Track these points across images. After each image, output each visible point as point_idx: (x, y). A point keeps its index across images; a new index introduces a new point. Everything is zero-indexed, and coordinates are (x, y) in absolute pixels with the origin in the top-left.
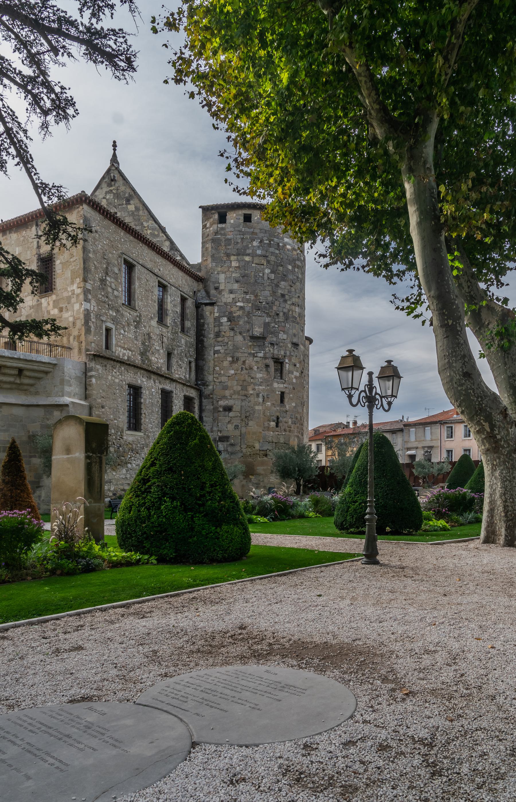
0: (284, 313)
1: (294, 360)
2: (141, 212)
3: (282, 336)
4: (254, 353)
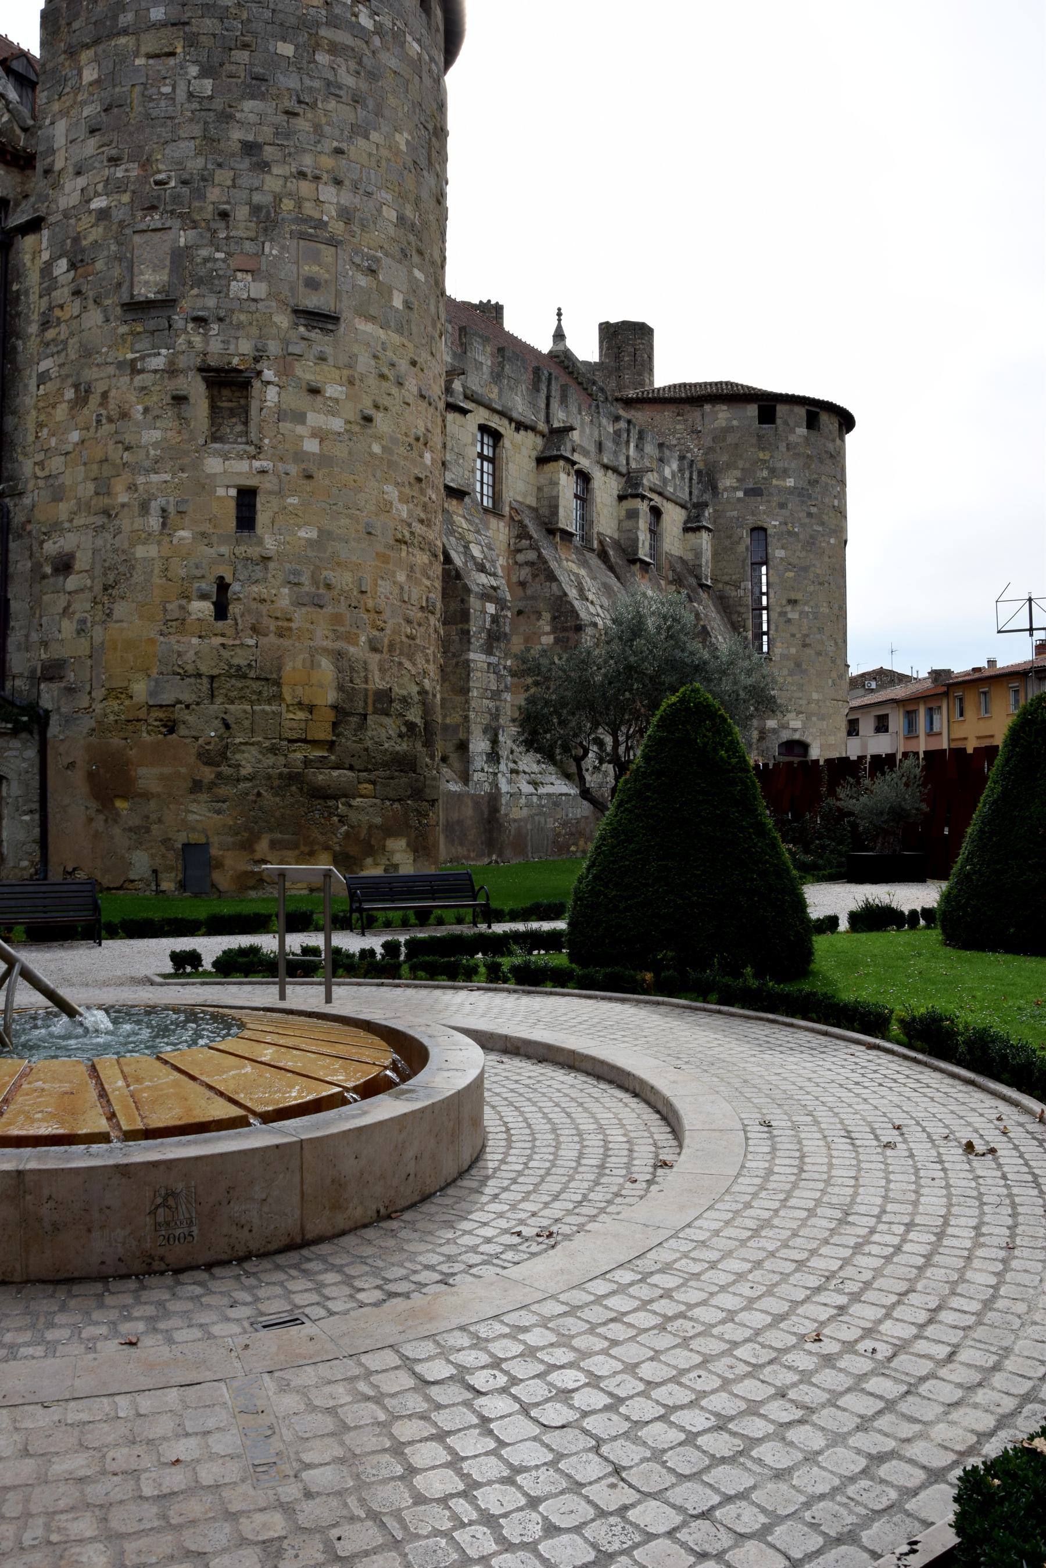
0: (256, 210)
1: (307, 372)
3: (242, 286)
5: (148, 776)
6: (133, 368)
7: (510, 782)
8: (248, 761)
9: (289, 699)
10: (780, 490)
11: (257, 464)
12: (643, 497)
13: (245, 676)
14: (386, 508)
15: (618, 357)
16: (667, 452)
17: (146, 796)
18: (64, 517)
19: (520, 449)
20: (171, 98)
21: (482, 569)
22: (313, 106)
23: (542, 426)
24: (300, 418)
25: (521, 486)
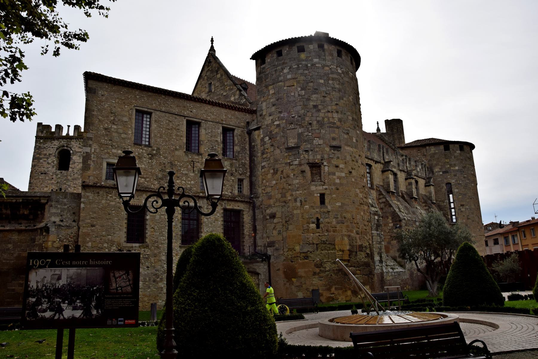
0: (318, 122)
1: (334, 162)
2: (224, 77)
4: (290, 162)
5: (301, 272)
6: (290, 164)
7: (386, 269)
8: (328, 266)
9: (337, 249)
10: (454, 171)
11: (324, 187)
12: (413, 178)
13: (326, 243)
14: (357, 195)
15: (392, 131)
16: (418, 163)
17: (301, 277)
18: (272, 203)
19: (377, 168)
20: (294, 96)
21: (372, 206)
22: (329, 94)
23: (382, 161)
24: (334, 174)
25: (378, 180)
